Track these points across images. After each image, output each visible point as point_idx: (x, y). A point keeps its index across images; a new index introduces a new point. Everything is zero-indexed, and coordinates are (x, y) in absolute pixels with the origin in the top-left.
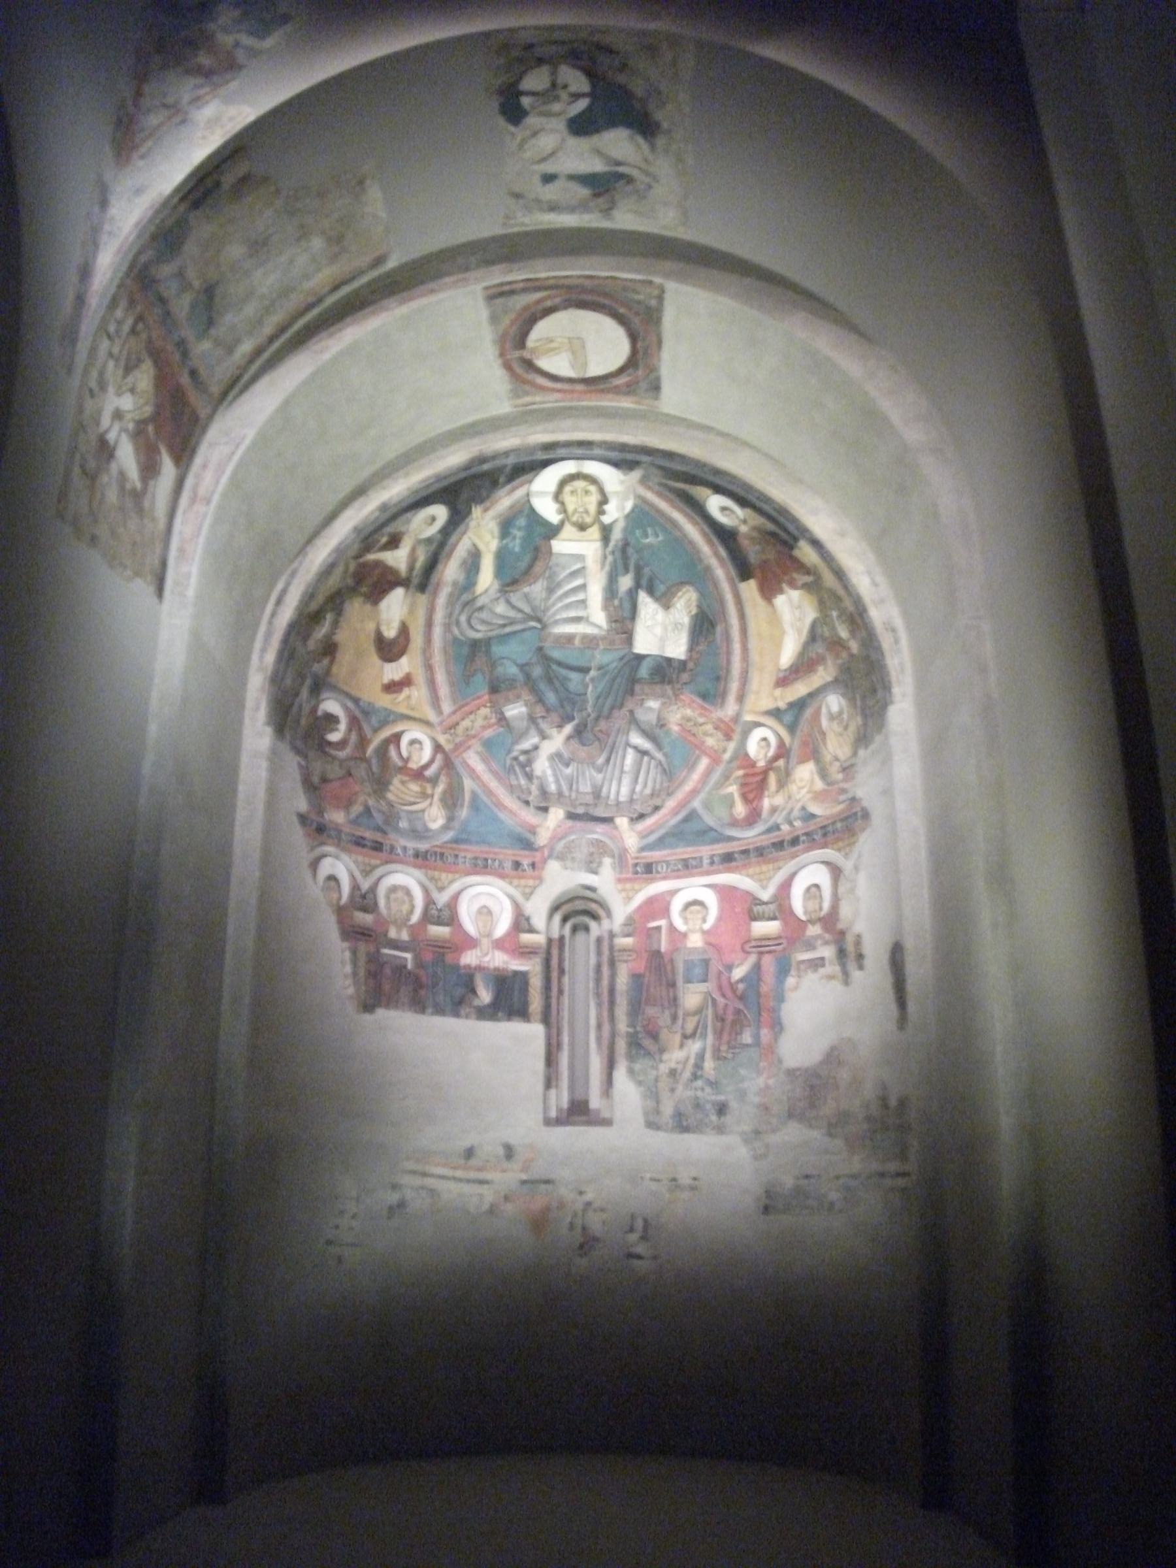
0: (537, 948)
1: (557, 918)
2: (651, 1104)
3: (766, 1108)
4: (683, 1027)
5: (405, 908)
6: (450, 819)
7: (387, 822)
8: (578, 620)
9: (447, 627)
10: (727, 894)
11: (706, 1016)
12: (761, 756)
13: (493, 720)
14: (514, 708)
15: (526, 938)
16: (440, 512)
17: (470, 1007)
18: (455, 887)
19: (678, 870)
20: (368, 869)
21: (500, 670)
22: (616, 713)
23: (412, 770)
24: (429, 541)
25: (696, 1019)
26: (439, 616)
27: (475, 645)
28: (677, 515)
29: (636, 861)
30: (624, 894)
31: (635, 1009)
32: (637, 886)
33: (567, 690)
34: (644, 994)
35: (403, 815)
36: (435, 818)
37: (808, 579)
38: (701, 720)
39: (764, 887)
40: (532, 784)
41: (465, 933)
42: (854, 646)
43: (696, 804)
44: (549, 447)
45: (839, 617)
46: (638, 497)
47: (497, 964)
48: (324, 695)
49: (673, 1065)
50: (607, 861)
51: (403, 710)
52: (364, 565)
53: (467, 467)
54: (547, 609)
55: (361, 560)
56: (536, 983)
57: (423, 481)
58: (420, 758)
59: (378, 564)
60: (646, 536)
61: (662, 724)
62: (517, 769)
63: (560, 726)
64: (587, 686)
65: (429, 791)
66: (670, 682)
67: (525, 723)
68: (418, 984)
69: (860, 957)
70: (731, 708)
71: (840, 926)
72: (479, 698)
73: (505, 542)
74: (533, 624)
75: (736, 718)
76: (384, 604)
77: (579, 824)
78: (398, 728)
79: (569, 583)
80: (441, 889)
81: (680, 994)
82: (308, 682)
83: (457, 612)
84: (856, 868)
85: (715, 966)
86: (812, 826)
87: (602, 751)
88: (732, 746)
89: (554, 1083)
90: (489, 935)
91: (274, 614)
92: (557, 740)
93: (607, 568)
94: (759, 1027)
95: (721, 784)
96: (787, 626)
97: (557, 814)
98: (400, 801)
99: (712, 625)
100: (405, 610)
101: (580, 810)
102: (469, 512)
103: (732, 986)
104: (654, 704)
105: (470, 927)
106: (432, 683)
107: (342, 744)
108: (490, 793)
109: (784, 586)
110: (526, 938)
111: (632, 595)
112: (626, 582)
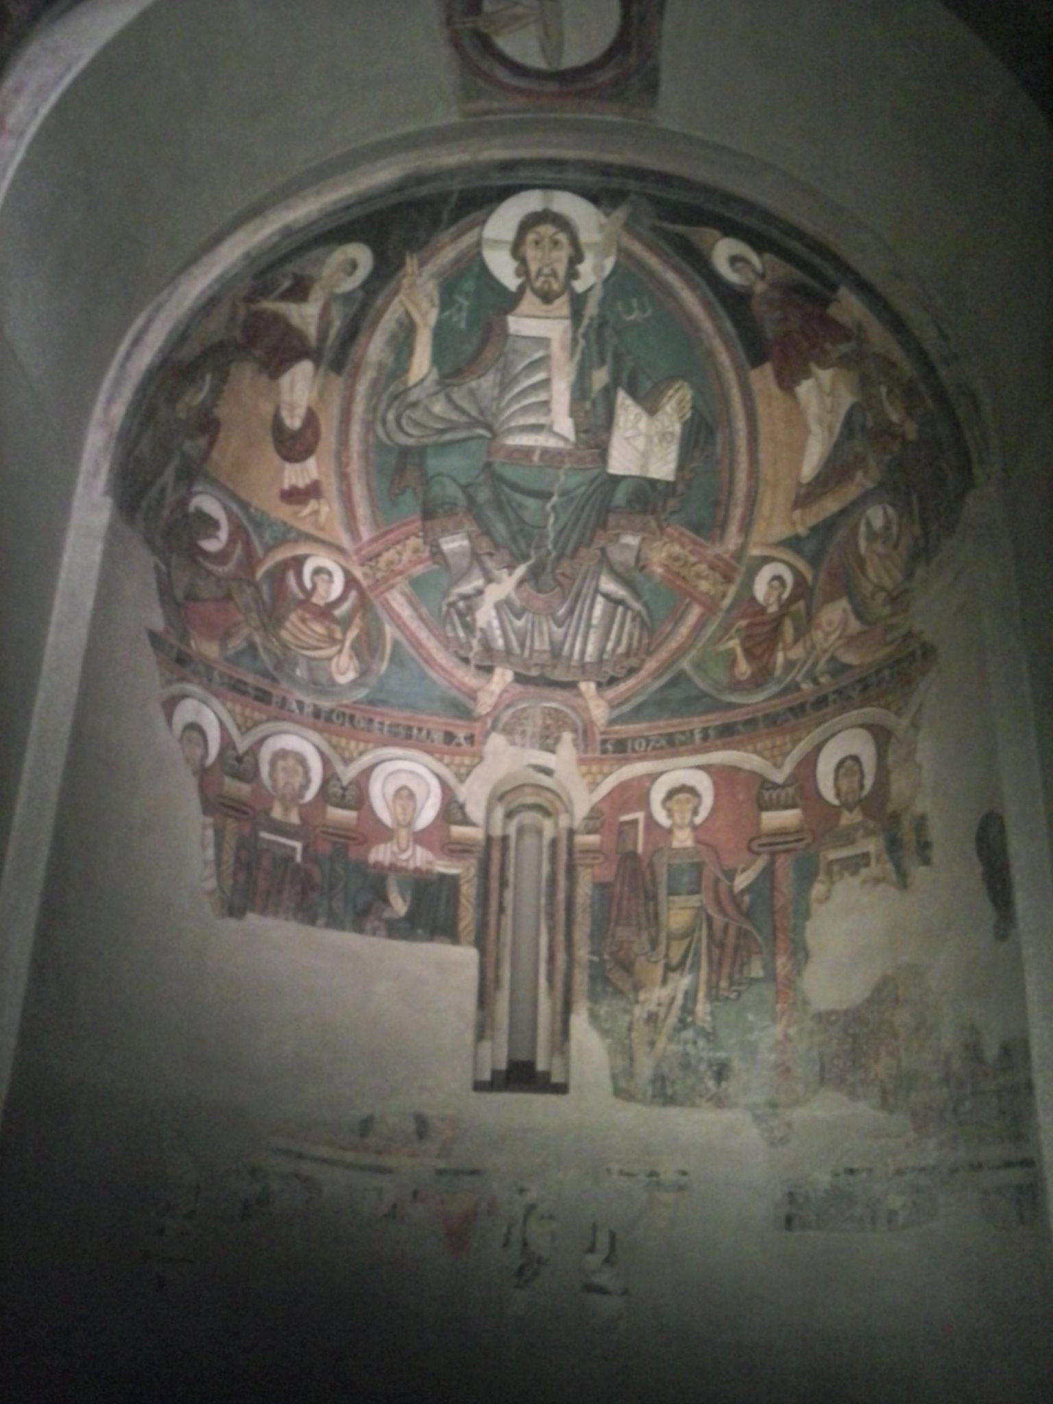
0: (472, 846)
1: (499, 812)
2: (621, 1063)
3: (785, 1070)
4: (666, 956)
5: (298, 781)
6: (363, 673)
7: (278, 666)
8: (537, 428)
9: (369, 427)
10: (724, 777)
11: (699, 940)
12: (773, 599)
13: (426, 554)
14: (453, 541)
15: (457, 831)
16: (362, 255)
17: (379, 919)
18: (366, 760)
19: (662, 748)
20: (249, 724)
21: (436, 490)
22: (583, 552)
23: (316, 605)
24: (347, 298)
25: (686, 942)
26: (359, 408)
27: (405, 452)
28: (671, 277)
29: (604, 737)
30: (589, 778)
31: (599, 932)
32: (606, 769)
33: (520, 519)
34: (615, 908)
35: (302, 662)
36: (344, 670)
37: (844, 348)
38: (693, 559)
39: (778, 766)
40: (474, 637)
41: (378, 821)
42: (911, 430)
43: (685, 664)
44: (507, 166)
45: (890, 392)
46: (624, 253)
47: (418, 864)
48: (198, 488)
49: (652, 1007)
50: (567, 737)
51: (307, 528)
52: (258, 315)
53: (400, 187)
54: (501, 411)
55: (254, 307)
56: (468, 891)
57: (335, 203)
58: (328, 592)
59: (277, 319)
60: (630, 311)
61: (641, 565)
62: (456, 618)
63: (511, 567)
64: (547, 517)
65: (338, 636)
66: (654, 512)
67: (465, 562)
68: (307, 886)
69: (924, 847)
70: (733, 540)
71: (890, 808)
72: (406, 524)
73: (447, 313)
74: (481, 431)
75: (739, 554)
76: (285, 380)
77: (532, 689)
78: (301, 550)
79: (528, 376)
80: (347, 761)
81: (663, 908)
82: (175, 463)
83: (383, 405)
84: (915, 726)
85: (711, 871)
86: (844, 681)
87: (564, 599)
88: (732, 590)
89: (488, 1032)
90: (409, 825)
91: (128, 356)
92: (505, 585)
93: (578, 357)
94: (774, 955)
95: (717, 639)
96: (815, 427)
97: (503, 677)
98: (299, 643)
99: (711, 432)
100: (315, 394)
101: (534, 672)
102: (401, 265)
103: (735, 899)
104: (631, 540)
105: (385, 816)
106: (347, 498)
107: (221, 557)
108: (418, 645)
109: (813, 367)
110: (457, 831)
111: (608, 394)
112: (600, 377)
